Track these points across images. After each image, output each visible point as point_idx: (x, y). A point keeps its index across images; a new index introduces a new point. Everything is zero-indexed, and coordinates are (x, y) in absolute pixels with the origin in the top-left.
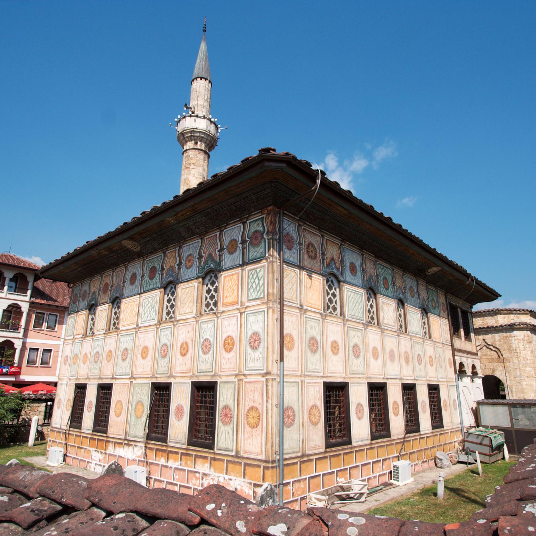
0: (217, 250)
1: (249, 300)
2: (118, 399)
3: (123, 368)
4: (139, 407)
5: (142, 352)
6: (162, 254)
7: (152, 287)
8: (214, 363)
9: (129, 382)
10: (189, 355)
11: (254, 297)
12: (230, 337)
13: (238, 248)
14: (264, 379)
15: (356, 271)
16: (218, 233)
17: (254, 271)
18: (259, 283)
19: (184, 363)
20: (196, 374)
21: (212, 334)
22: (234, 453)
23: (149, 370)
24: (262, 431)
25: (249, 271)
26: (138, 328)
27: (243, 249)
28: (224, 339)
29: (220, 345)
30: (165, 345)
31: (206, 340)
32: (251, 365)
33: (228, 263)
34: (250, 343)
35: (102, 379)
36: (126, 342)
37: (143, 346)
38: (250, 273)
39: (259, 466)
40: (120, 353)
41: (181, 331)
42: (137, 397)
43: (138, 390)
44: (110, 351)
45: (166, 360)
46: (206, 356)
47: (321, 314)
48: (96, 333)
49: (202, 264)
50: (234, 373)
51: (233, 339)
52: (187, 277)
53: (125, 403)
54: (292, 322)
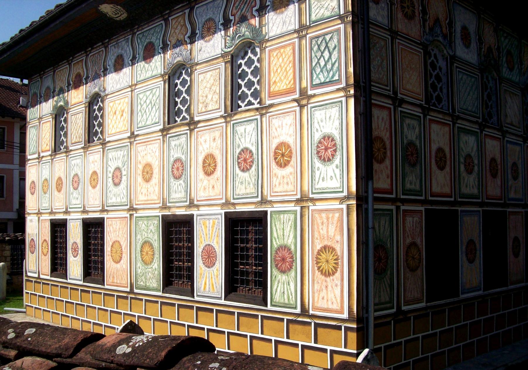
0: (254, 9)
2: (114, 239)
3: (117, 195)
4: (147, 249)
5: (143, 172)
6: (163, 22)
7: (149, 74)
8: (260, 185)
9: (128, 216)
10: (219, 173)
11: (323, 80)
15: (470, 40)
17: (320, 39)
19: (211, 187)
20: (232, 201)
21: (254, 139)
22: (298, 311)
23: (156, 198)
24: (342, 280)
25: (311, 39)
26: (133, 136)
28: (274, 146)
30: (178, 160)
31: (245, 150)
32: (321, 185)
34: (318, 152)
35: (87, 212)
36: (116, 158)
37: (144, 162)
38: (314, 42)
39: (339, 328)
40: (110, 175)
41: (203, 138)
42: (142, 235)
43: (142, 225)
44: (95, 173)
45: (181, 182)
46: (246, 174)
47: (420, 106)
48: (70, 148)
50: (294, 198)
51: (289, 147)
53: (124, 244)
54: (383, 119)
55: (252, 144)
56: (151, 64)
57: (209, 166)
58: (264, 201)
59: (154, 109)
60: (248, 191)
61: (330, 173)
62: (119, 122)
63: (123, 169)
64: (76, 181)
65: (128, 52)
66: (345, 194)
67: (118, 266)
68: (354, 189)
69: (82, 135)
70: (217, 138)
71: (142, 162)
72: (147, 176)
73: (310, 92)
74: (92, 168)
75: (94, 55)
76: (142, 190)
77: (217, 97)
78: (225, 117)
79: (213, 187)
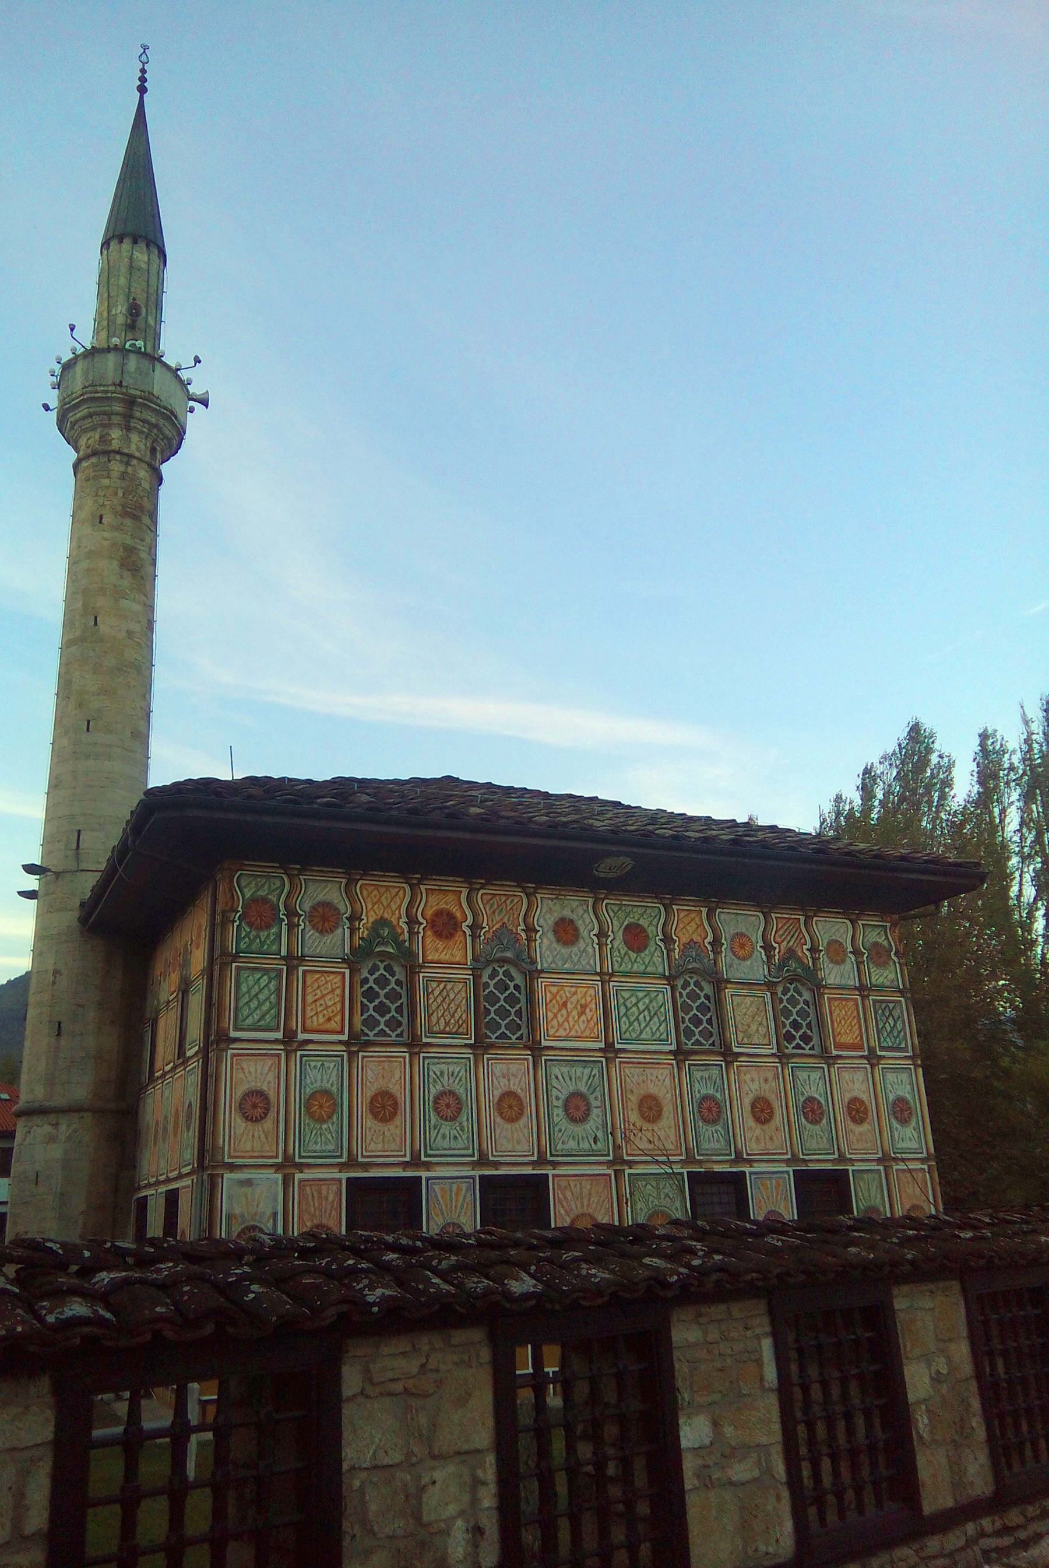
0: (805, 947)
1: (882, 1048)
9: (611, 1172)
12: (854, 1100)
13: (848, 961)
14: (925, 1167)
16: (802, 918)
18: (895, 1024)
25: (875, 1002)
28: (847, 1100)
31: (811, 1100)
33: (832, 976)
34: (894, 1113)
38: (877, 1005)
41: (748, 1076)
45: (719, 1128)
46: (817, 1128)
55: (820, 1095)
56: (642, 955)
57: (762, 1110)
58: (842, 1159)
59: (656, 1019)
60: (821, 1146)
62: (577, 1022)
63: (591, 1098)
64: (448, 1106)
65: (588, 921)
66: (925, 1155)
68: (932, 1150)
69: (466, 1021)
70: (770, 1080)
71: (635, 1091)
73: (879, 1053)
77: (765, 1030)
78: (778, 1057)
79: (771, 1139)
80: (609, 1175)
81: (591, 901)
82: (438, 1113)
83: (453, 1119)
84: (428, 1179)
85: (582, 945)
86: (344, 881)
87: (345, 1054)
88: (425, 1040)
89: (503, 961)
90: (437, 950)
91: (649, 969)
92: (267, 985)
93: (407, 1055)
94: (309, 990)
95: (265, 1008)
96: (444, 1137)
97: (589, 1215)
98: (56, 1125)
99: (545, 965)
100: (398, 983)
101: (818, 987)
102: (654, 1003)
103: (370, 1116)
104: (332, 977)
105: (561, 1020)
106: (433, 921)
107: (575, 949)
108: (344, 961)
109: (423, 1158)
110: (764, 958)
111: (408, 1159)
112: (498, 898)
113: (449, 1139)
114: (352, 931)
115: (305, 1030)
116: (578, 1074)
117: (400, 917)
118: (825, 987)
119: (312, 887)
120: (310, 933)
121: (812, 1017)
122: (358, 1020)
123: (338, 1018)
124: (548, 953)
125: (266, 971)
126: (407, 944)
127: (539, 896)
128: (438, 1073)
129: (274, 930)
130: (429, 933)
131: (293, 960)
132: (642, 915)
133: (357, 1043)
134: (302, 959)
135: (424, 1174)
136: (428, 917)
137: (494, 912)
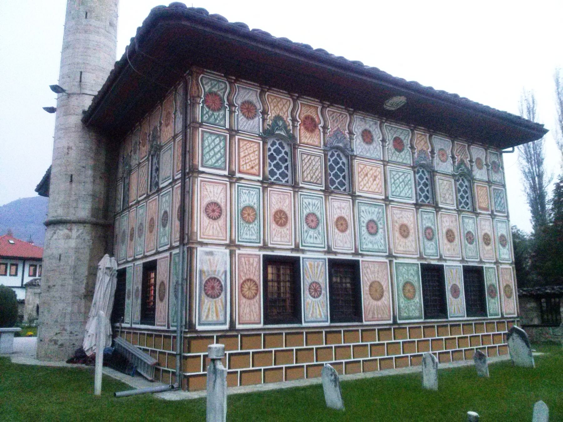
1: (496, 211)
2: (372, 279)
7: (400, 160)
12: (486, 235)
14: (511, 267)
16: (467, 145)
22: (500, 316)
25: (494, 189)
26: (386, 199)
27: (488, 170)
28: (483, 234)
29: (481, 240)
31: (469, 233)
32: (503, 256)
43: (403, 269)
45: (433, 243)
46: (471, 246)
49: (456, 164)
50: (493, 261)
52: (441, 169)
56: (402, 154)
58: (481, 262)
59: (407, 187)
61: (505, 252)
62: (372, 184)
63: (379, 223)
64: (312, 221)
67: (379, 303)
68: (514, 260)
69: (321, 177)
72: (406, 233)
73: (495, 213)
74: (337, 214)
75: (334, 112)
76: (401, 243)
80: (386, 262)
81: (379, 122)
82: (308, 224)
83: (315, 228)
84: (303, 258)
85: (374, 144)
86: (259, 91)
87: (261, 188)
88: (301, 185)
89: (338, 148)
90: (306, 137)
91: (404, 162)
92: (218, 144)
93: (292, 192)
94: (241, 150)
95: (218, 156)
96: (311, 237)
97: (378, 282)
98: (71, 230)
99: (358, 153)
100: (286, 153)
101: (472, 180)
102: (406, 179)
103: (274, 222)
104: (253, 144)
105: (365, 182)
106: (304, 121)
107: (371, 146)
108: (260, 136)
109: (301, 247)
110: (452, 162)
111: (293, 247)
112: (335, 114)
113: (312, 239)
114: (264, 120)
115: (240, 172)
116: (373, 211)
117: (288, 117)
118: (475, 179)
119: (242, 91)
120: (241, 117)
121: (469, 194)
122: (268, 169)
123: (257, 167)
124: (359, 147)
125: (219, 136)
126: (291, 132)
127: (355, 116)
128: (307, 203)
129: (222, 112)
130: (302, 127)
131: (233, 132)
132: (401, 133)
133: (266, 183)
134: (237, 132)
135: (301, 255)
136: (302, 118)
137: (334, 121)
